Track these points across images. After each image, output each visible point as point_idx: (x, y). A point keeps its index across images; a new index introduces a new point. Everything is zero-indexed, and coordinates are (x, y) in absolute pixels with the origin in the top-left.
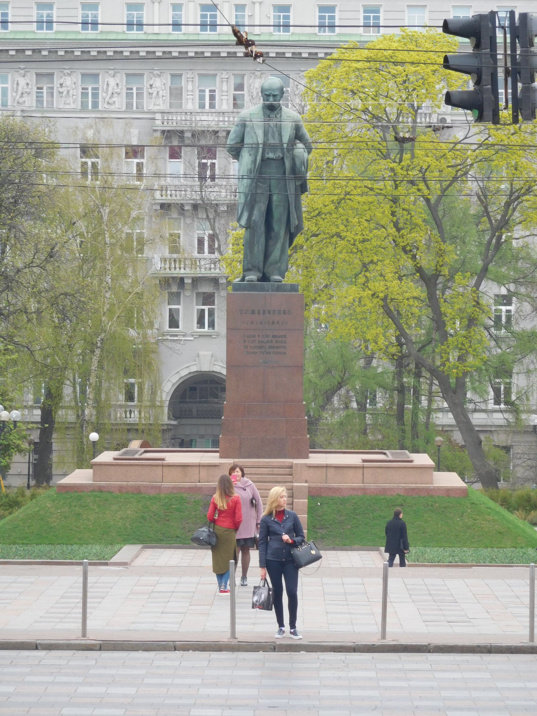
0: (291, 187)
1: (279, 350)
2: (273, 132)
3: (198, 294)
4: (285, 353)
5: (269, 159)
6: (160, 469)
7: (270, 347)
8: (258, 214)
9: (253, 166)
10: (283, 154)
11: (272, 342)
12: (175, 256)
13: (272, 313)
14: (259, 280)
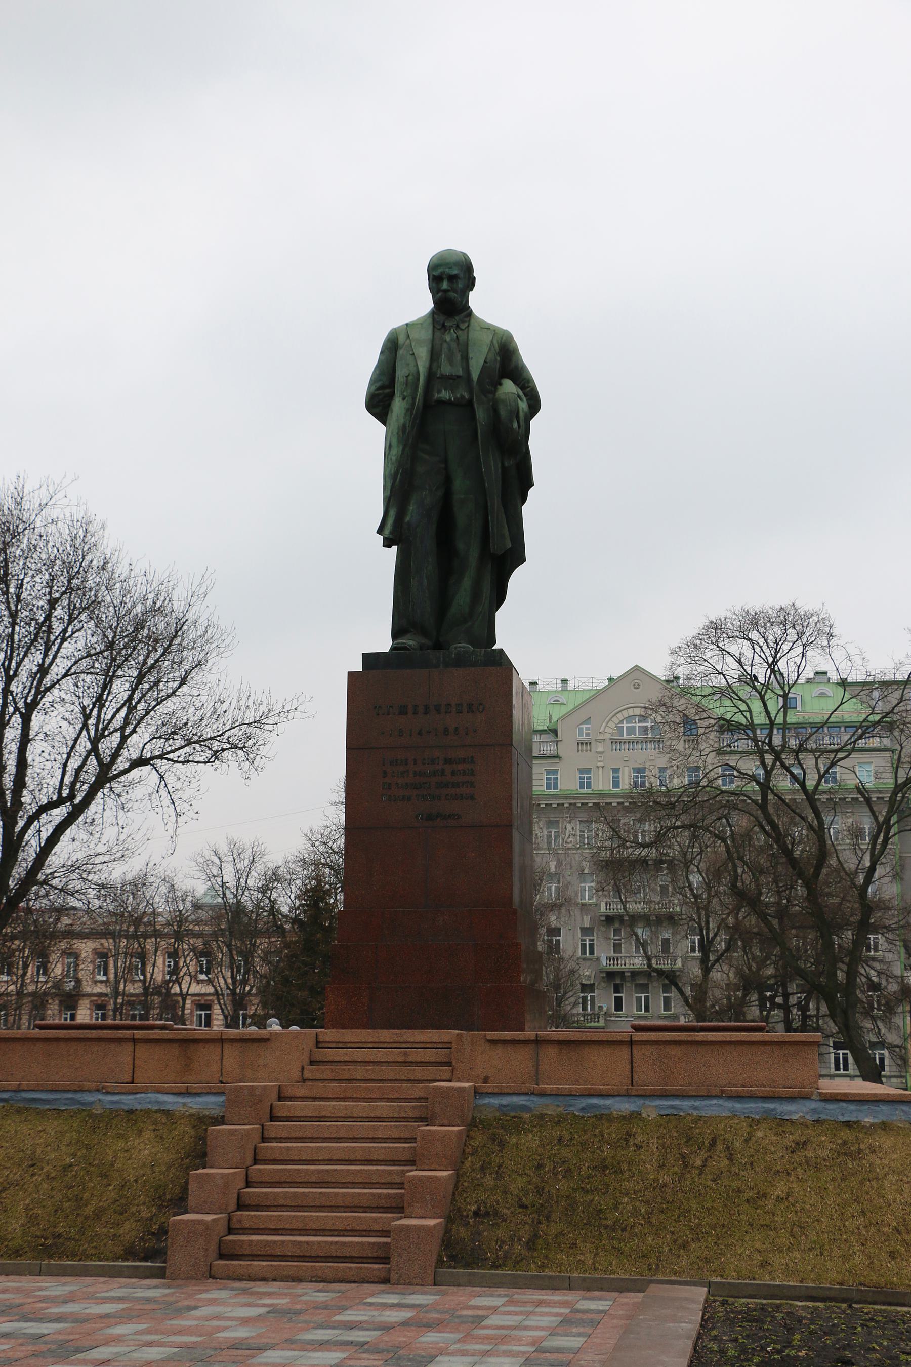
0: (492, 465)
2: (450, 349)
3: (636, 985)
4: (472, 798)
5: (441, 402)
6: (129, 1047)
9: (408, 418)
10: (471, 392)
11: (443, 772)
12: (616, 955)
14: (422, 647)
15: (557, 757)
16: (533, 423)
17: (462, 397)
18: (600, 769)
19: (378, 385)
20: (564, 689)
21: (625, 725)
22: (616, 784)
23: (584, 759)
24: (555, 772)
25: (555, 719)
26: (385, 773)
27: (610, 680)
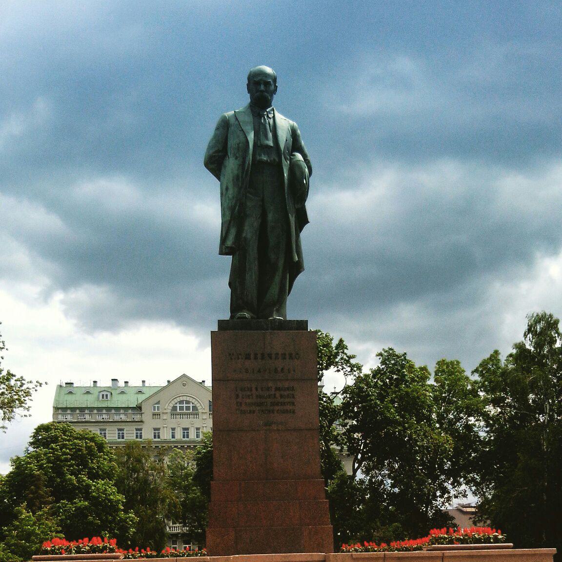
1: (285, 408)
4: (294, 412)
5: (262, 162)
7: (273, 404)
8: (250, 230)
13: (273, 356)
15: (142, 422)
16: (311, 179)
17: (274, 160)
18: (165, 428)
19: (216, 149)
20: (144, 386)
21: (178, 405)
22: (173, 437)
23: (157, 423)
24: (141, 430)
25: (140, 401)
26: (237, 396)
27: (169, 381)
